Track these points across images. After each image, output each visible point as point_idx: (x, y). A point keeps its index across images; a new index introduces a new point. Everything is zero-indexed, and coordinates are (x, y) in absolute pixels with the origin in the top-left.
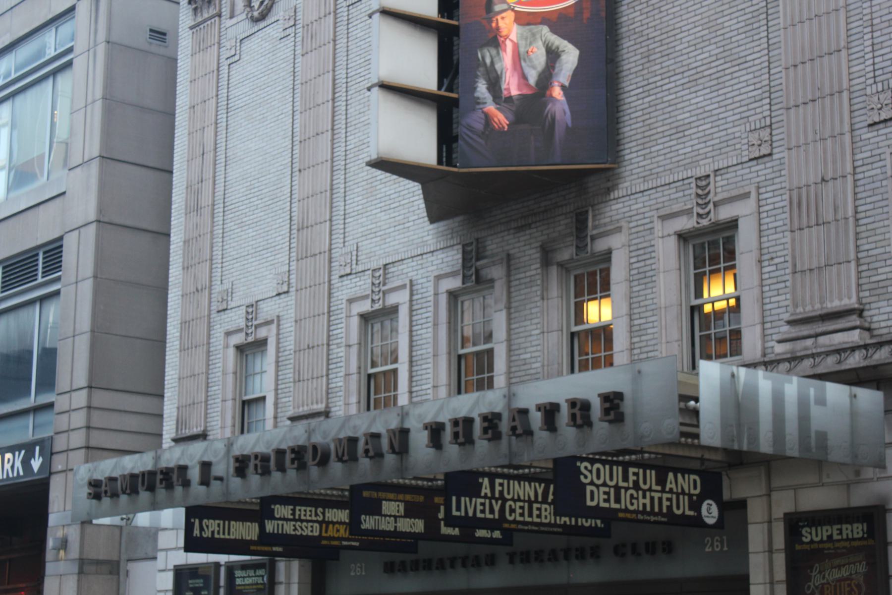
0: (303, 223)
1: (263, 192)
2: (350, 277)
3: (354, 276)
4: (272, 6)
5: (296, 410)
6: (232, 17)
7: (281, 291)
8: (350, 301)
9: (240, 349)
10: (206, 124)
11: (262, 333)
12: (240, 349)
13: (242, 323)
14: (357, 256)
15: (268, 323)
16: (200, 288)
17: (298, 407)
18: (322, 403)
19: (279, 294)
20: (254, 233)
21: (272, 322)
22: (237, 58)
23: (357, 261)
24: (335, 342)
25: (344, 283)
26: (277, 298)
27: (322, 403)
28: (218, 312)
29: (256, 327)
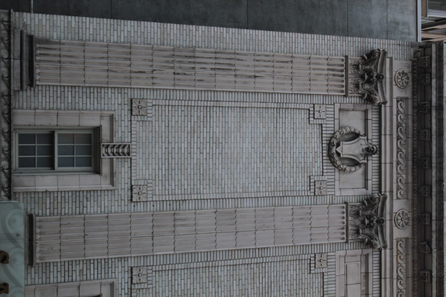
0: (180, 220)
1: (211, 160)
2: (130, 279)
3: (129, 287)
4: (334, 165)
5: (38, 224)
6: (340, 110)
7: (135, 191)
8: (112, 285)
9: (97, 130)
10: (276, 81)
11: (105, 169)
12: (97, 130)
13: (117, 140)
14: (143, 289)
15: (112, 174)
16: (155, 74)
17: (40, 227)
18: (41, 259)
19: (132, 190)
20: (183, 152)
21: (112, 183)
22: (311, 119)
23: (139, 289)
24: (85, 265)
25: (126, 273)
26: (129, 185)
27: (41, 259)
28: (131, 100)
29: (112, 159)
